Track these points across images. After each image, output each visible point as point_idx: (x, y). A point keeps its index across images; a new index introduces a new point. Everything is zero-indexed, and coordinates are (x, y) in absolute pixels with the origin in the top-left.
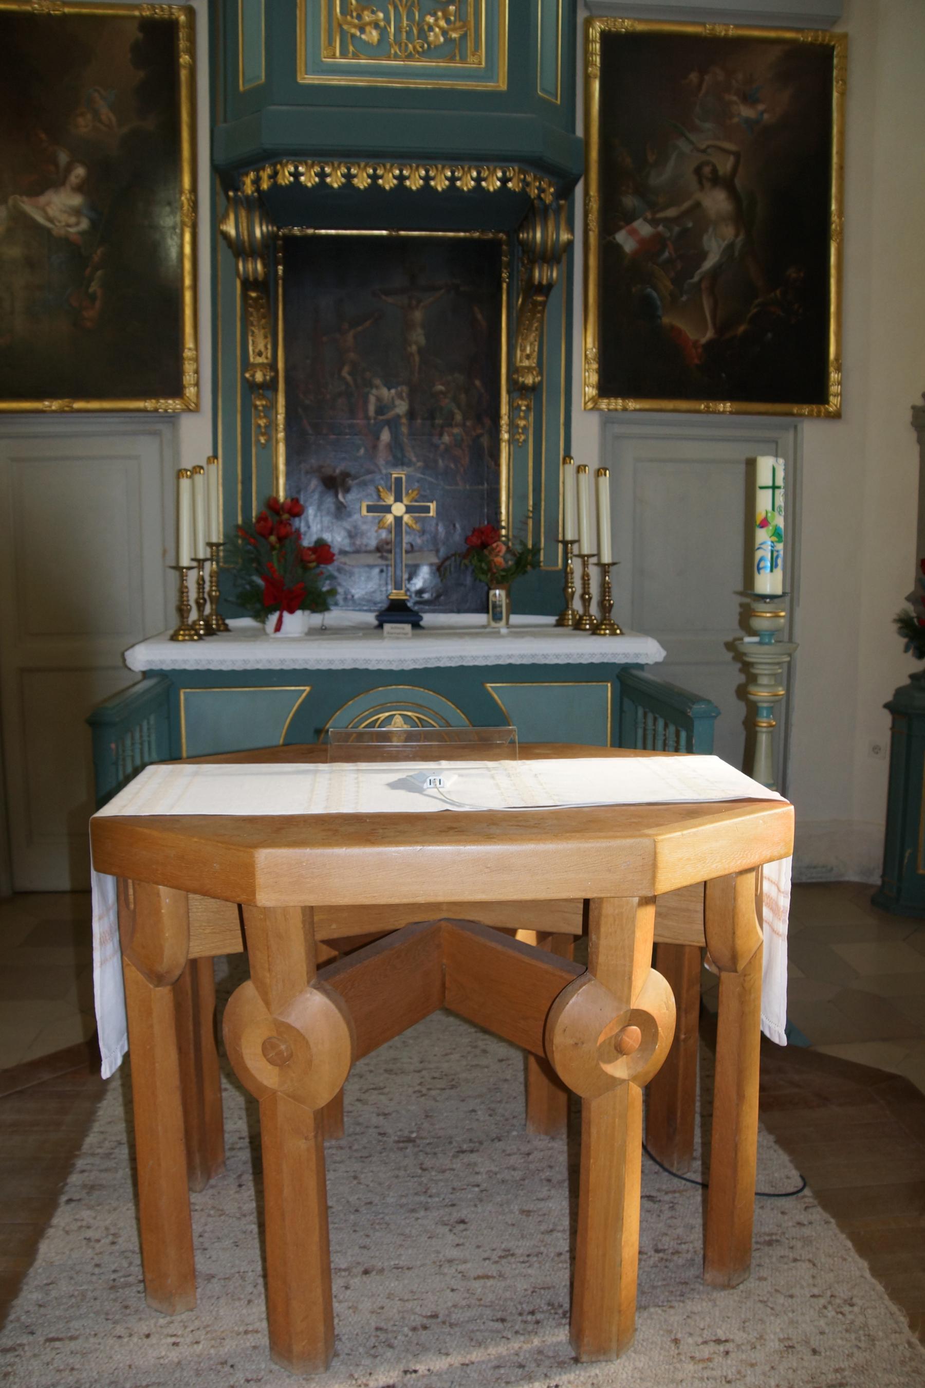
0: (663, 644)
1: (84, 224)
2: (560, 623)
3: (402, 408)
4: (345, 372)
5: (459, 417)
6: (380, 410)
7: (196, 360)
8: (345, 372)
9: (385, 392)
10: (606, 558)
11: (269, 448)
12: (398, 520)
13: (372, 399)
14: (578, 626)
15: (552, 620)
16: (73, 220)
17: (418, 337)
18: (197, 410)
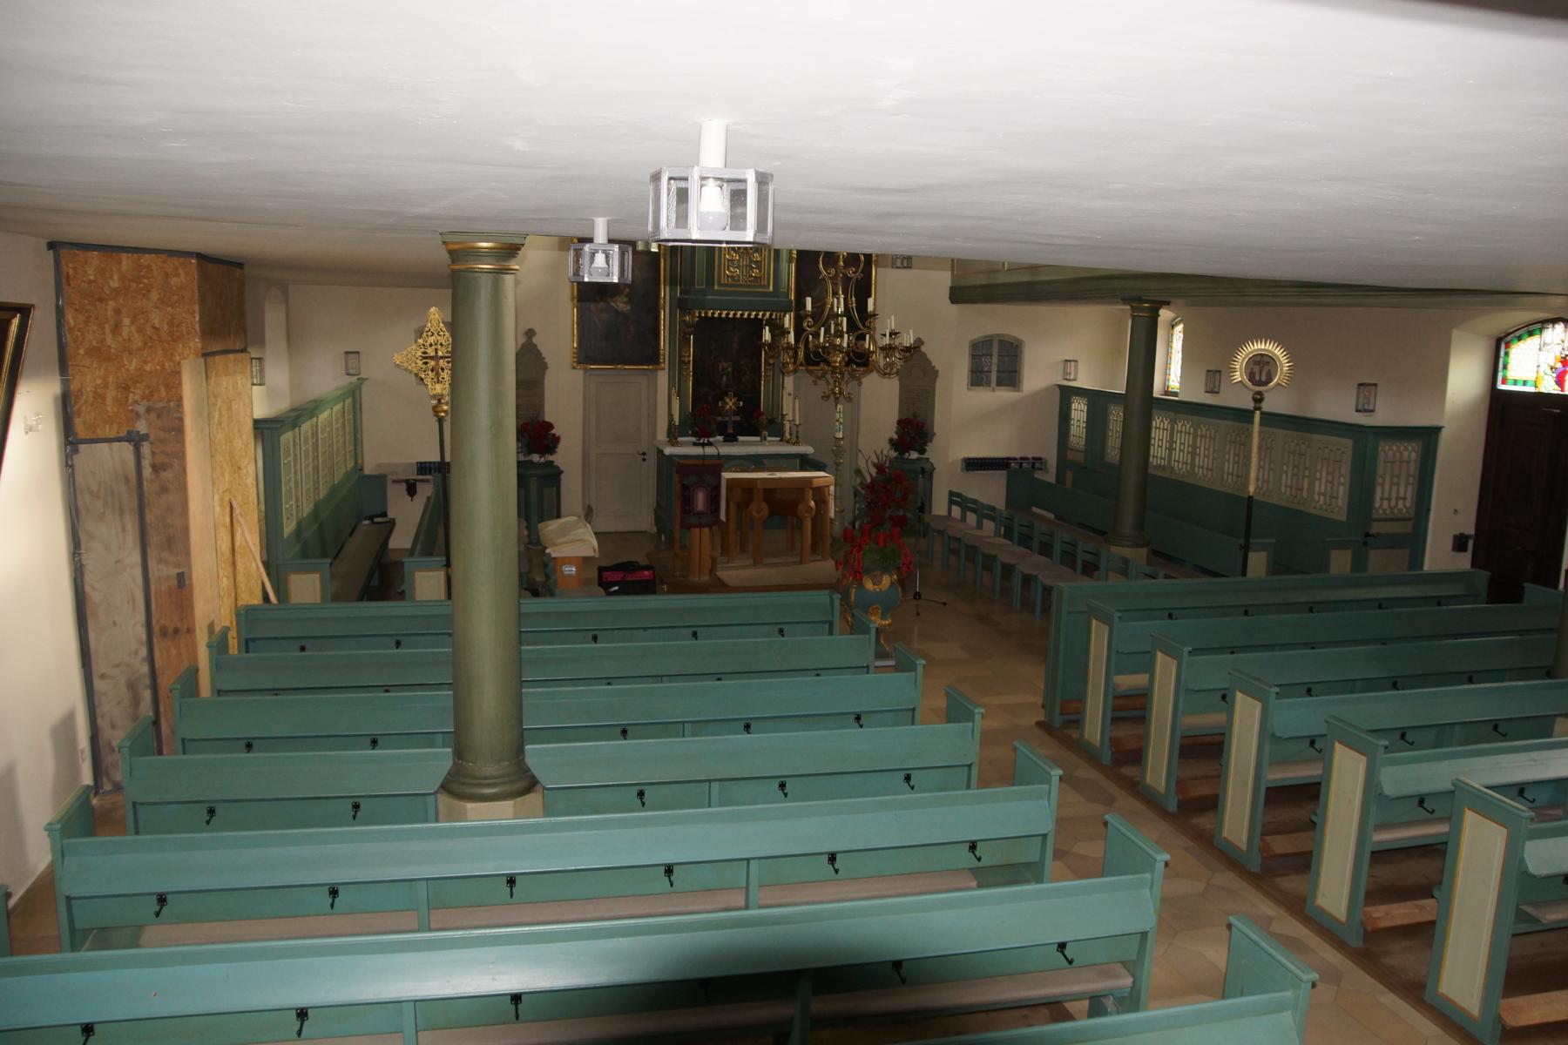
0: (814, 448)
1: (629, 308)
2: (781, 440)
3: (730, 369)
4: (712, 357)
5: (748, 373)
6: (723, 368)
7: (664, 355)
8: (712, 357)
9: (725, 364)
10: (797, 423)
11: (687, 381)
12: (731, 407)
13: (720, 367)
14: (788, 442)
15: (778, 439)
16: (624, 306)
17: (735, 346)
18: (663, 369)
